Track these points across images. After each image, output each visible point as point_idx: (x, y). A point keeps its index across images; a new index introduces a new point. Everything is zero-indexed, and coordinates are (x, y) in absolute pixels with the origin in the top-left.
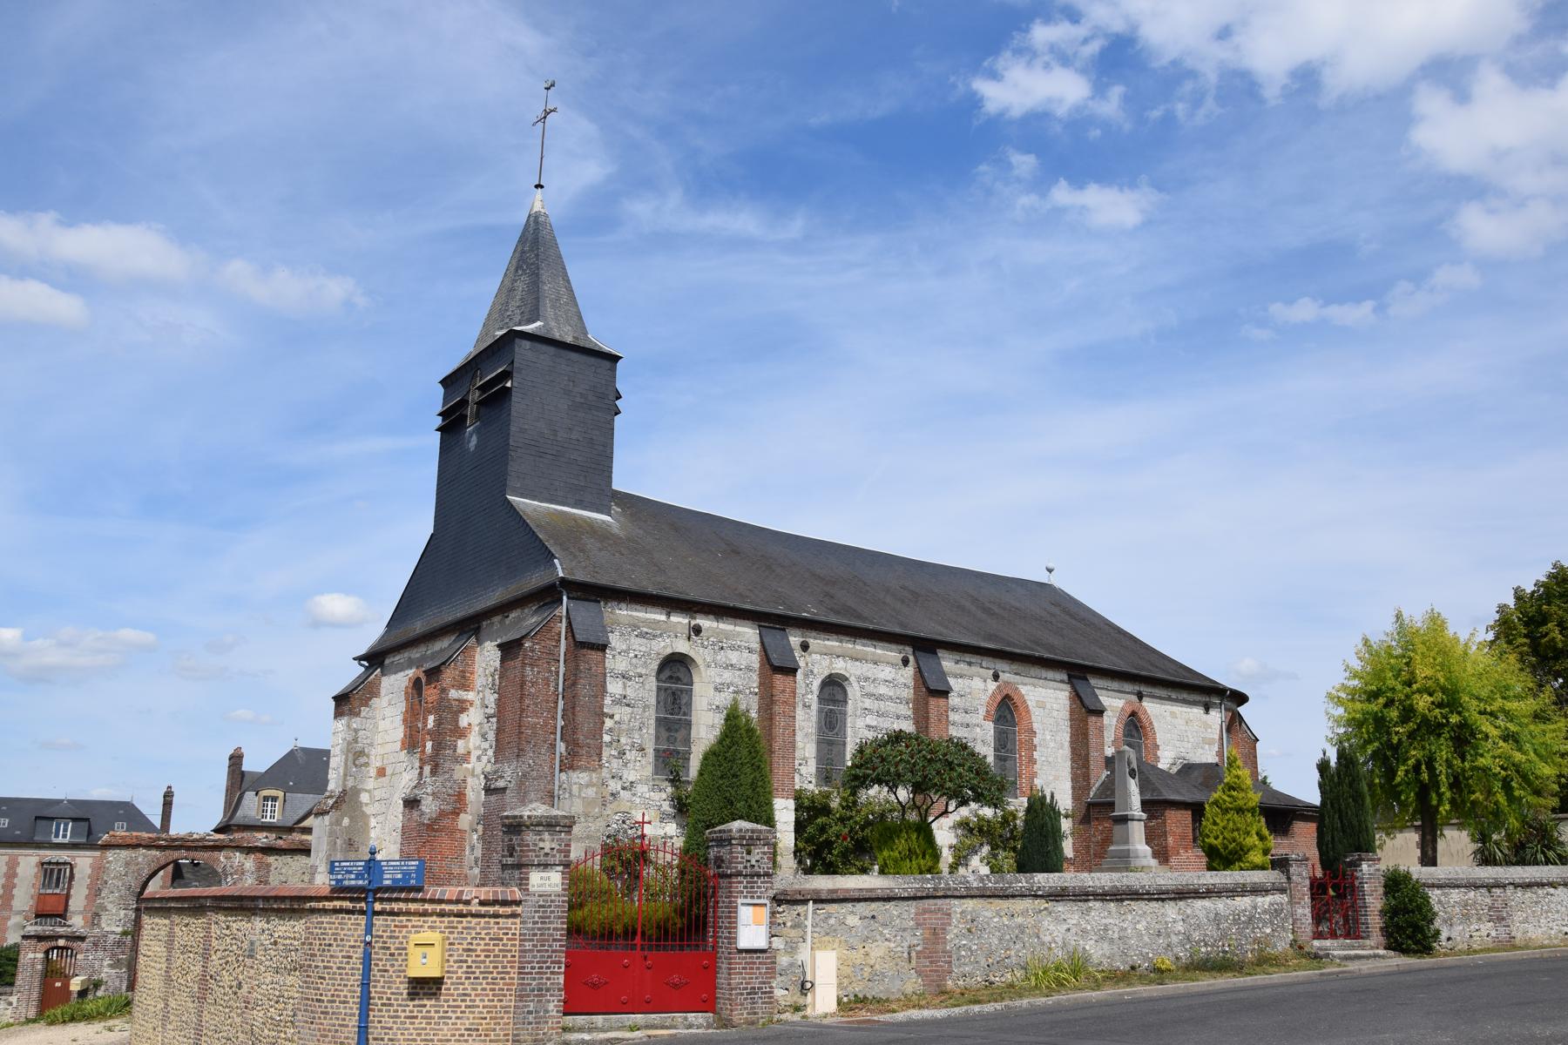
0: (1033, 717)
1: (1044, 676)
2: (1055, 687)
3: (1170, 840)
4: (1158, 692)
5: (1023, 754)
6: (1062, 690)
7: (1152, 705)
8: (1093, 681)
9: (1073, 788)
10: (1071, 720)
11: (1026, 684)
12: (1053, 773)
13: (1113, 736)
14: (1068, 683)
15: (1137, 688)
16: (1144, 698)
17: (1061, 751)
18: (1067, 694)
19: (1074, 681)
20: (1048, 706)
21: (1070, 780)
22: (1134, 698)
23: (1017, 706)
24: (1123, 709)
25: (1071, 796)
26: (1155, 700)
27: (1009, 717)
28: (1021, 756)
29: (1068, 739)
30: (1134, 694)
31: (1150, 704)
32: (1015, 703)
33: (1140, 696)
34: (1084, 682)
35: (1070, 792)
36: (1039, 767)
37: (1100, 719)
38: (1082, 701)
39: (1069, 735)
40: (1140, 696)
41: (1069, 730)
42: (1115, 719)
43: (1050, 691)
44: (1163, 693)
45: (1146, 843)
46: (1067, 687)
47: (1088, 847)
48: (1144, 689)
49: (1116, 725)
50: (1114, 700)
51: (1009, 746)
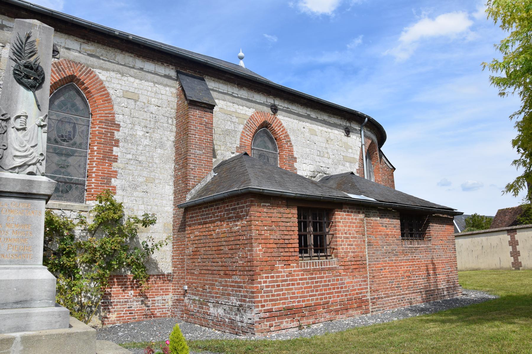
0: (115, 107)
1: (165, 83)
2: (155, 80)
3: (258, 250)
4: (294, 108)
5: (95, 148)
6: (166, 85)
7: (289, 119)
8: (211, 84)
9: (175, 193)
10: (177, 118)
11: (107, 70)
12: (145, 173)
13: (238, 142)
14: (176, 80)
15: (270, 101)
16: (279, 112)
17: (159, 151)
18: (174, 91)
19: (182, 77)
20: (143, 99)
21: (172, 183)
22: (268, 110)
23: (89, 92)
24: (251, 118)
25: (172, 203)
26: (292, 116)
27: (81, 106)
28: (93, 151)
29: (172, 138)
30: (267, 106)
31: (285, 118)
32: (86, 88)
33: (275, 109)
34: (203, 81)
35: (172, 197)
36: (121, 165)
37: (208, 115)
38: (185, 95)
39: (174, 134)
40: (275, 109)
41: (174, 129)
42: (242, 126)
43: (147, 83)
44: (302, 111)
45: (45, 262)
46: (177, 84)
47: (183, 260)
48: (278, 103)
49: (243, 132)
50: (241, 107)
51: (77, 139)
